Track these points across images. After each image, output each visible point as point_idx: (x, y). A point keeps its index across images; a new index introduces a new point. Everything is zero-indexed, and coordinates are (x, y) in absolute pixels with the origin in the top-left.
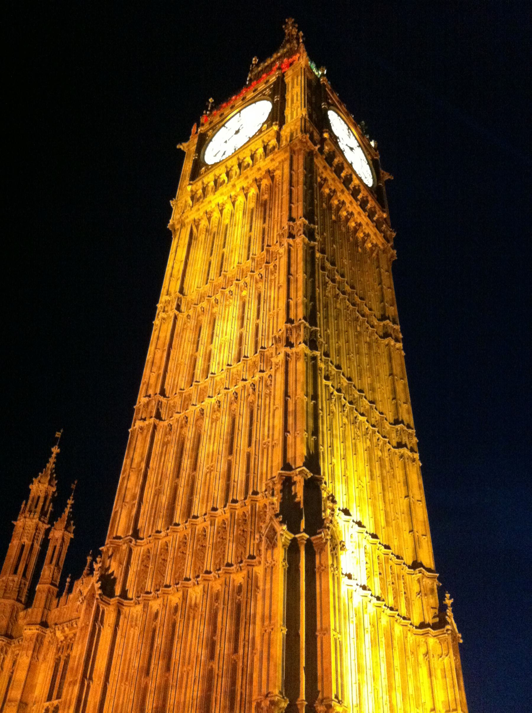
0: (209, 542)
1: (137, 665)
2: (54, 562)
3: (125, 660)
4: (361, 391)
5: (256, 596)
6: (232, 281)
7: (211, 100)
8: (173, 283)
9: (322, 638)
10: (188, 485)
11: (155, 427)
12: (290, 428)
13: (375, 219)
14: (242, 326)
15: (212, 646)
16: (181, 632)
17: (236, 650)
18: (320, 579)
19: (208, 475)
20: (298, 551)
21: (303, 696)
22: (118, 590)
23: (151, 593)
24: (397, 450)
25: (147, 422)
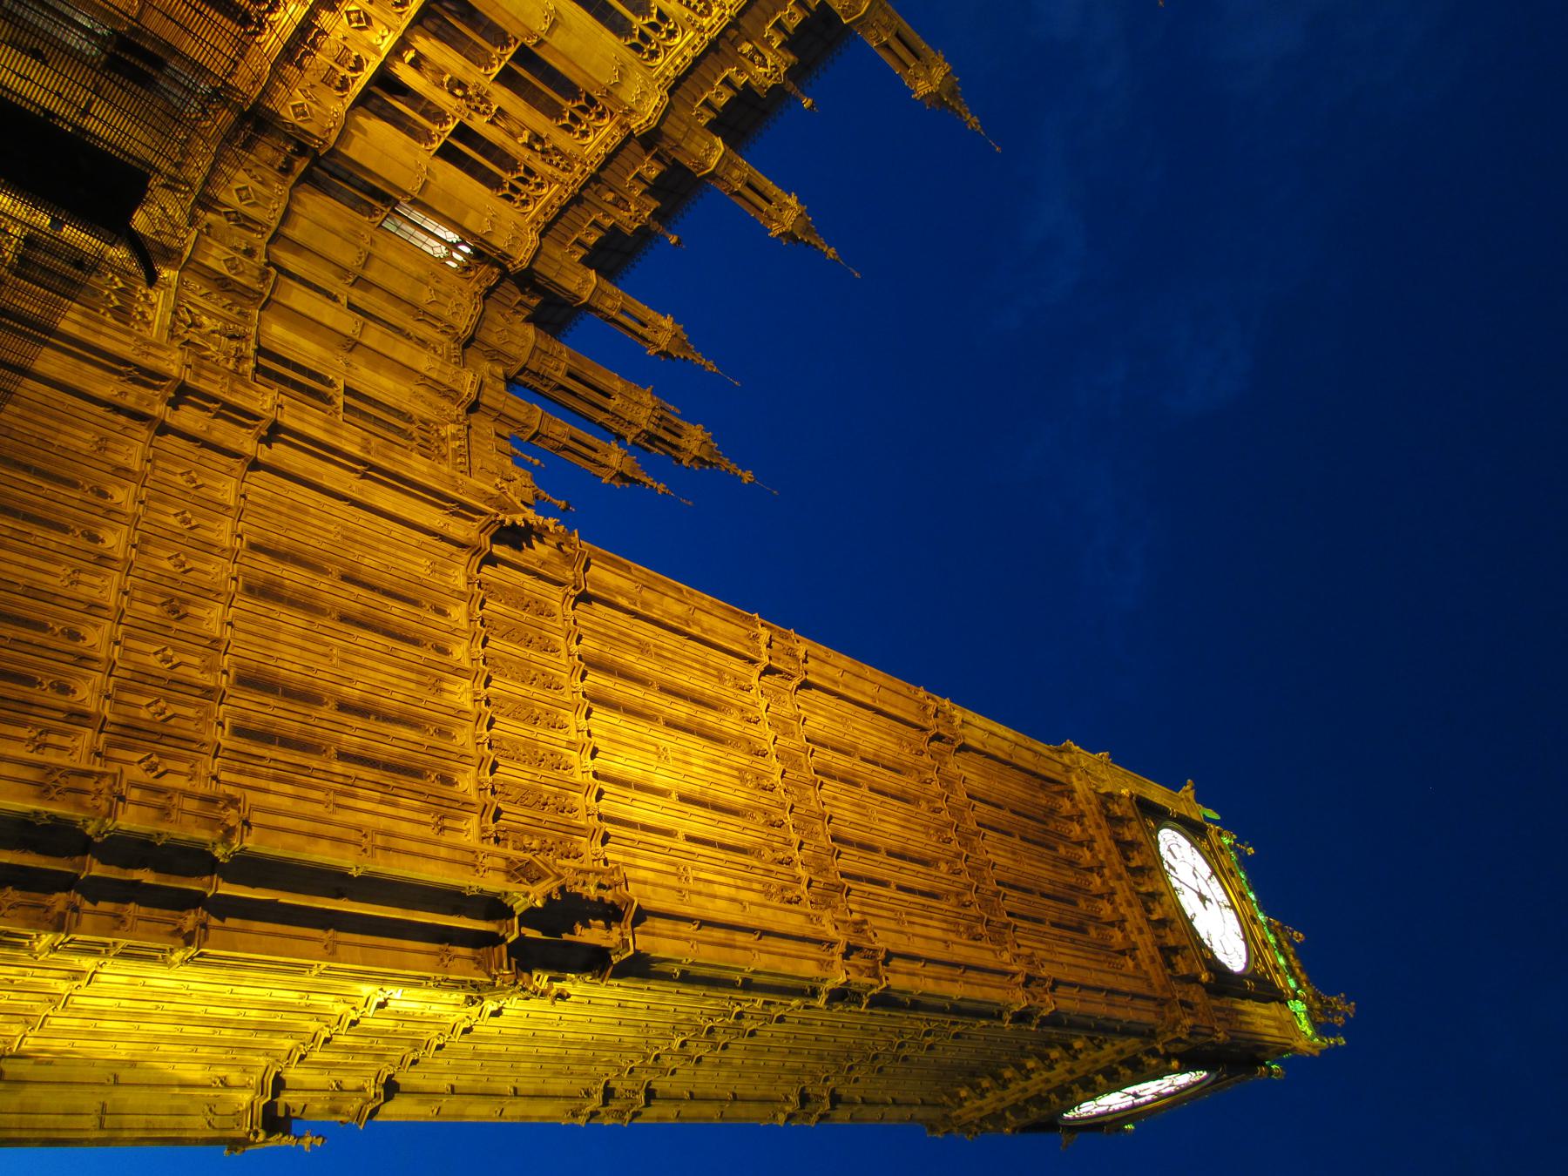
0: (542, 734)
1: (366, 561)
2: (571, 444)
3: (379, 540)
4: (725, 1047)
5: (427, 812)
6: (965, 845)
7: (1251, 851)
8: (978, 733)
9: (321, 941)
10: (644, 706)
11: (752, 662)
12: (707, 933)
13: (1008, 1114)
14: (890, 854)
15: (362, 711)
16: (402, 655)
17: (344, 756)
18: (428, 953)
19: (653, 749)
20: (488, 917)
21: (226, 889)
22: (500, 551)
23: (481, 608)
24: (601, 1086)
25: (764, 648)
